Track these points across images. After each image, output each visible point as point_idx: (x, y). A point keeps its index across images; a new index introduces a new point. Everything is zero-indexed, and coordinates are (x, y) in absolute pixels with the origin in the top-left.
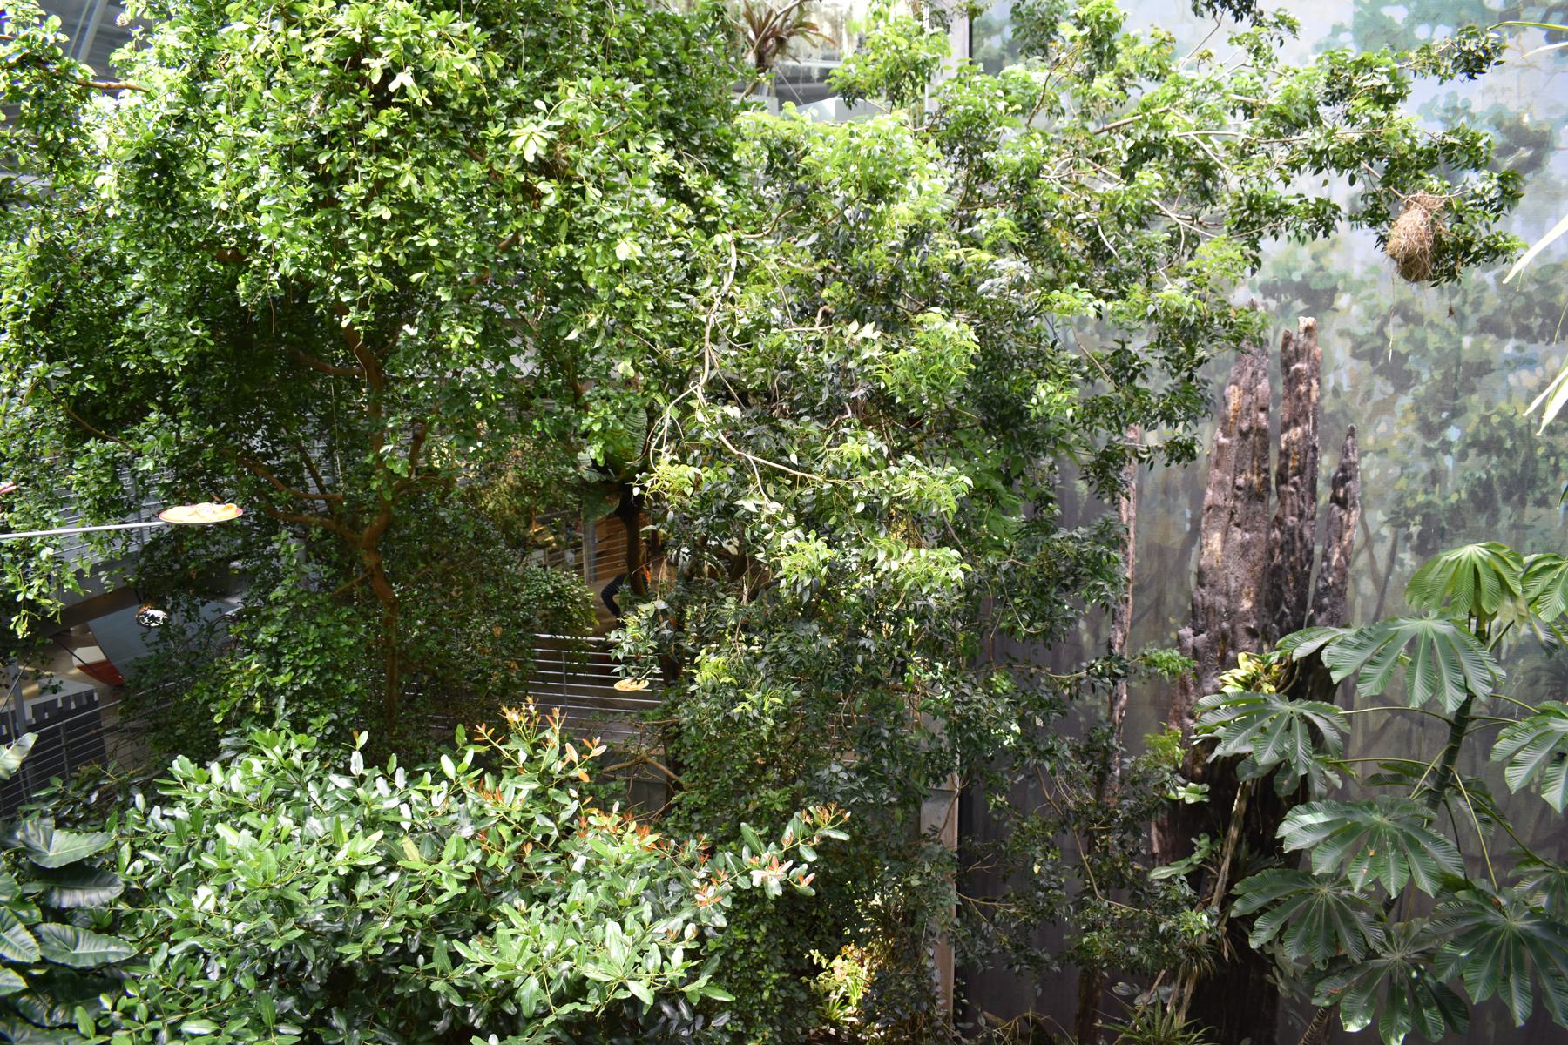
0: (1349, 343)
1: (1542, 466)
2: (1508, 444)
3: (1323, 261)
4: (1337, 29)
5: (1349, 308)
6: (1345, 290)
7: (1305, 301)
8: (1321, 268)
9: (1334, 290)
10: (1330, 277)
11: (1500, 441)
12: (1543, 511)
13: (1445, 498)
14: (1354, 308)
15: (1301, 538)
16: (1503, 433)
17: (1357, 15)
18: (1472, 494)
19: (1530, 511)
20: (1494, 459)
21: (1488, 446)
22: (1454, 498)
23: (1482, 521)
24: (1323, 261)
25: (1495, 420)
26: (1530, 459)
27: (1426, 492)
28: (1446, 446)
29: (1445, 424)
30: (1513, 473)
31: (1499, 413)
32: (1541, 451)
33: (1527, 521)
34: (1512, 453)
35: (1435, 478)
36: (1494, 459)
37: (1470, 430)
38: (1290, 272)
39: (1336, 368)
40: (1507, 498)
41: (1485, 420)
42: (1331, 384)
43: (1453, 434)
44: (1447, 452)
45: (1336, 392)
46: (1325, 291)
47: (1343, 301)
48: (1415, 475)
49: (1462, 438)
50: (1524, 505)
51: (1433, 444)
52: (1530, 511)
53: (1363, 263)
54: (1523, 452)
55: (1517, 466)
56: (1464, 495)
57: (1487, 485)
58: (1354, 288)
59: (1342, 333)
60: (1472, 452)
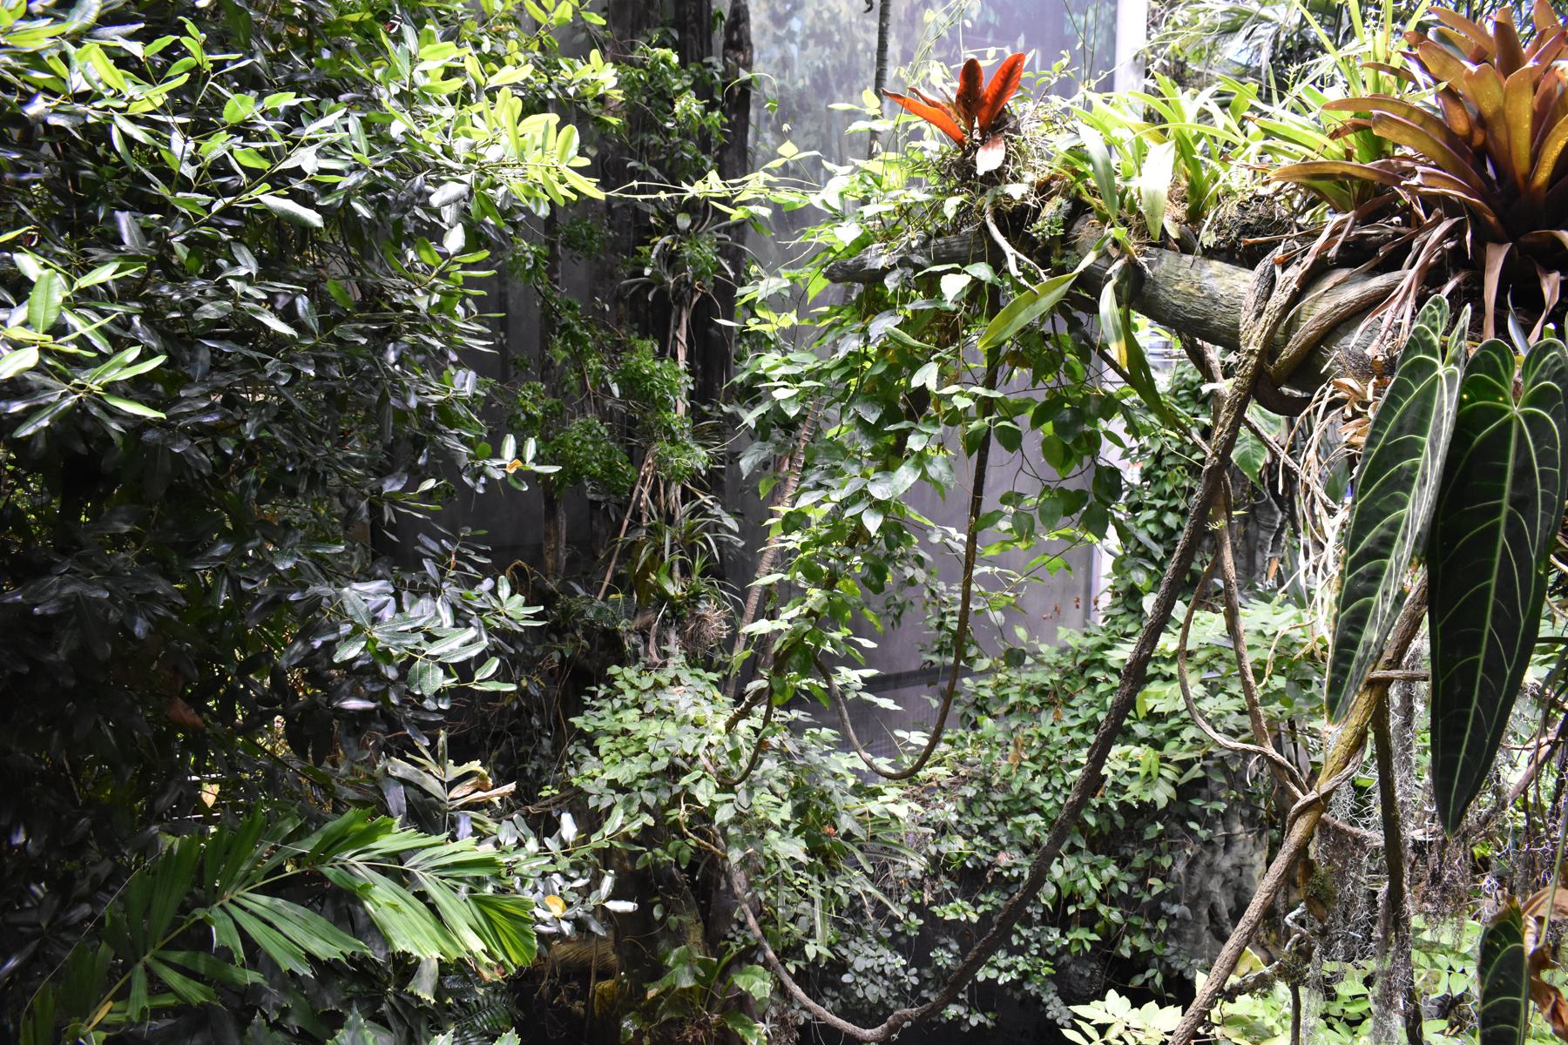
1: (862, 59)
2: (837, 38)
11: (830, 34)
13: (794, 83)
16: (833, 28)
18: (814, 81)
20: (828, 51)
21: (822, 38)
22: (800, 84)
25: (826, 15)
27: (779, 77)
28: (791, 36)
29: (789, 15)
30: (841, 64)
31: (829, 10)
32: (860, 46)
34: (839, 46)
35: (785, 63)
36: (828, 51)
37: (808, 22)
41: (818, 14)
43: (795, 24)
44: (792, 41)
48: (770, 60)
49: (803, 29)
51: (782, 33)
54: (847, 46)
56: (808, 82)
57: (823, 73)
60: (811, 43)
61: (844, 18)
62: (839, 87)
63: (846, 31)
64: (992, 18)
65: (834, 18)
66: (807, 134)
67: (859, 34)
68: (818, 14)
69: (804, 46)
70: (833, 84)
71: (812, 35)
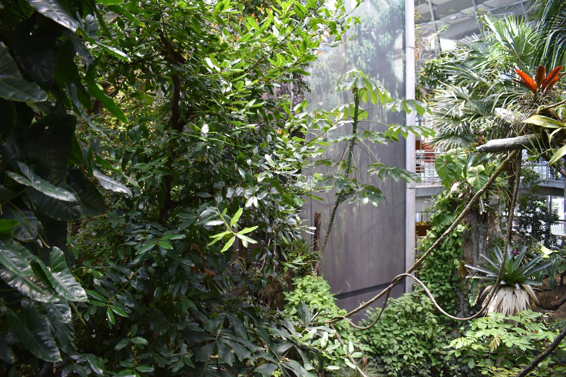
2: (323, 75)
11: (321, 73)
12: (332, 95)
15: (287, 89)
16: (322, 71)
18: (316, 89)
19: (329, 95)
21: (318, 75)
23: (319, 97)
25: (320, 67)
26: (328, 79)
31: (320, 65)
32: (330, 77)
33: (329, 98)
34: (324, 77)
40: (324, 91)
41: (317, 67)
50: (327, 92)
52: (329, 95)
54: (326, 77)
55: (325, 81)
57: (319, 86)
60: (315, 76)
61: (325, 68)
62: (324, 91)
63: (325, 72)
64: (369, 68)
65: (322, 68)
66: (315, 107)
67: (330, 73)
68: (317, 67)
69: (313, 77)
70: (322, 90)
71: (315, 74)
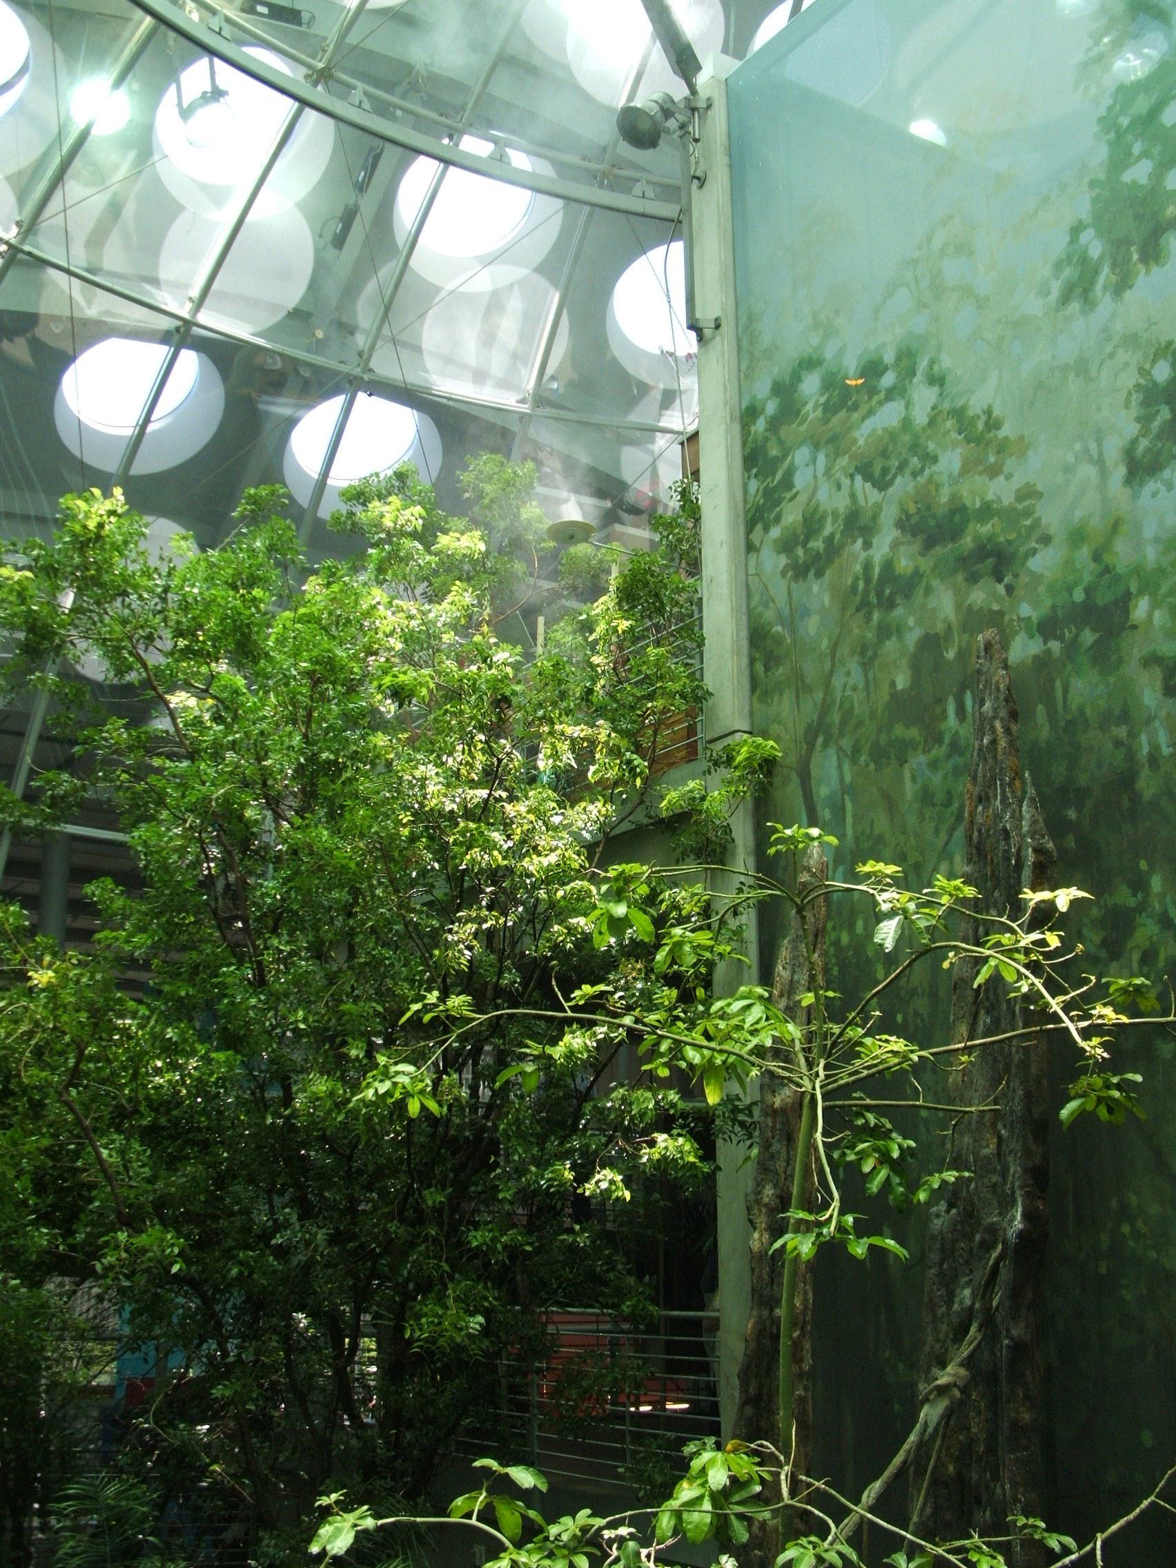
0: (1158, 673)
3: (1107, 559)
4: (1076, 231)
5: (1150, 615)
6: (1141, 592)
7: (1094, 630)
8: (1107, 570)
9: (1128, 596)
10: (1118, 578)
14: (1157, 615)
17: (1095, 201)
24: (1107, 559)
38: (1070, 590)
39: (1149, 721)
42: (1145, 750)
45: (1154, 760)
46: (1116, 603)
47: (1141, 609)
53: (1157, 540)
58: (1149, 582)
59: (1151, 660)
